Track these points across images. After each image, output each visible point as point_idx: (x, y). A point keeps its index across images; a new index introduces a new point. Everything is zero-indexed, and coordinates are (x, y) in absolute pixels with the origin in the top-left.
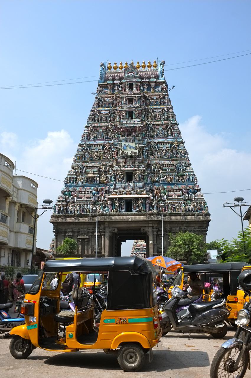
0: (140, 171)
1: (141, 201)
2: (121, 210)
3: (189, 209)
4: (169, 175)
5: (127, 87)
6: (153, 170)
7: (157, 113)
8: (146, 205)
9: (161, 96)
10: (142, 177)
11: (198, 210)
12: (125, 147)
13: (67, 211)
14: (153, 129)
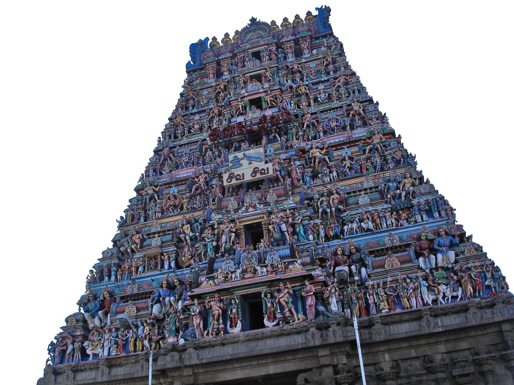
0: (281, 214)
1: (286, 290)
2: (231, 326)
3: (444, 293)
4: (366, 212)
5: (247, 59)
6: (320, 210)
7: (320, 90)
8: (303, 299)
9: (327, 60)
10: (291, 230)
11: (475, 291)
12: (237, 163)
13: (85, 356)
14: (313, 124)
